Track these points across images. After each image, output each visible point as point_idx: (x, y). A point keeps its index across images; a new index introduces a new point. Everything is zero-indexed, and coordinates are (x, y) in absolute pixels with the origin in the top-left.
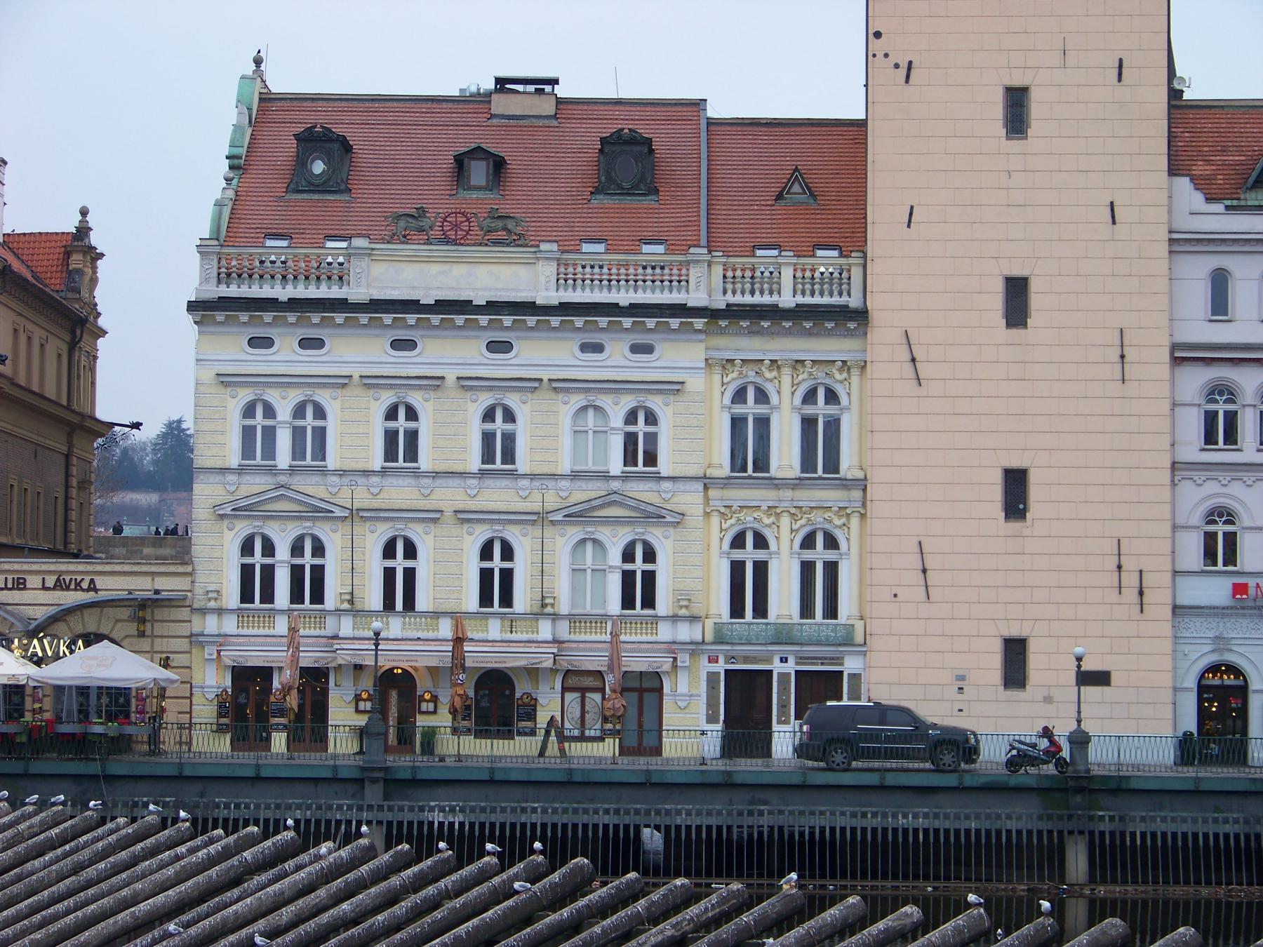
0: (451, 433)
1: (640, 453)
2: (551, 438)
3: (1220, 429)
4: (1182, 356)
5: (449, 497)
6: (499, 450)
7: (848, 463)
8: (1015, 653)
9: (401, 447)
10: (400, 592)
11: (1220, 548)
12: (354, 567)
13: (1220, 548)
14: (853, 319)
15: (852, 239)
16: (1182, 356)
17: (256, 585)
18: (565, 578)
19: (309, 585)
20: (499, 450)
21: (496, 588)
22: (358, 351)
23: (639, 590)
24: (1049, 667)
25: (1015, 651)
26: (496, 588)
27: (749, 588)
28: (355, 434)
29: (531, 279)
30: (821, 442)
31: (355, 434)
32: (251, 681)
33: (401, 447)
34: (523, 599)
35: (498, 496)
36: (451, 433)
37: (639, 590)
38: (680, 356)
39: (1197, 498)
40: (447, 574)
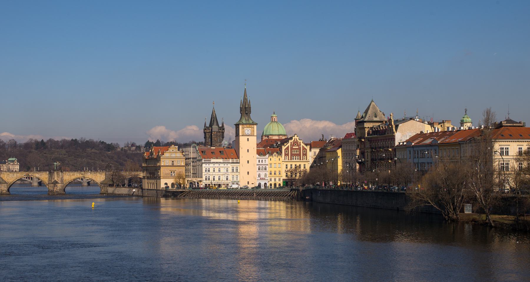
0: (217, 170)
1: (227, 171)
2: (223, 170)
3: (259, 169)
4: (257, 165)
5: (217, 174)
6: (219, 171)
7: (239, 171)
8: (248, 182)
9: (214, 171)
10: (214, 179)
11: (259, 176)
12: (211, 178)
13: (259, 176)
14: (239, 163)
15: (239, 158)
16: (257, 165)
17: (206, 179)
18: (223, 178)
19: (209, 179)
20: (219, 171)
21: (219, 179)
22: (211, 165)
23: (227, 179)
24: (250, 183)
25: (248, 182)
26: (219, 179)
27: (233, 178)
28: (211, 170)
29: (221, 160)
30: (237, 170)
31: (211, 170)
32: (206, 185)
33: (214, 171)
34: (221, 179)
35: (220, 173)
36: (217, 170)
37: (227, 179)
38: (229, 165)
39: (258, 173)
40: (217, 178)
